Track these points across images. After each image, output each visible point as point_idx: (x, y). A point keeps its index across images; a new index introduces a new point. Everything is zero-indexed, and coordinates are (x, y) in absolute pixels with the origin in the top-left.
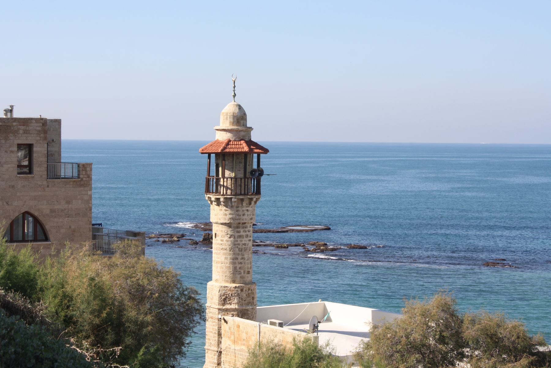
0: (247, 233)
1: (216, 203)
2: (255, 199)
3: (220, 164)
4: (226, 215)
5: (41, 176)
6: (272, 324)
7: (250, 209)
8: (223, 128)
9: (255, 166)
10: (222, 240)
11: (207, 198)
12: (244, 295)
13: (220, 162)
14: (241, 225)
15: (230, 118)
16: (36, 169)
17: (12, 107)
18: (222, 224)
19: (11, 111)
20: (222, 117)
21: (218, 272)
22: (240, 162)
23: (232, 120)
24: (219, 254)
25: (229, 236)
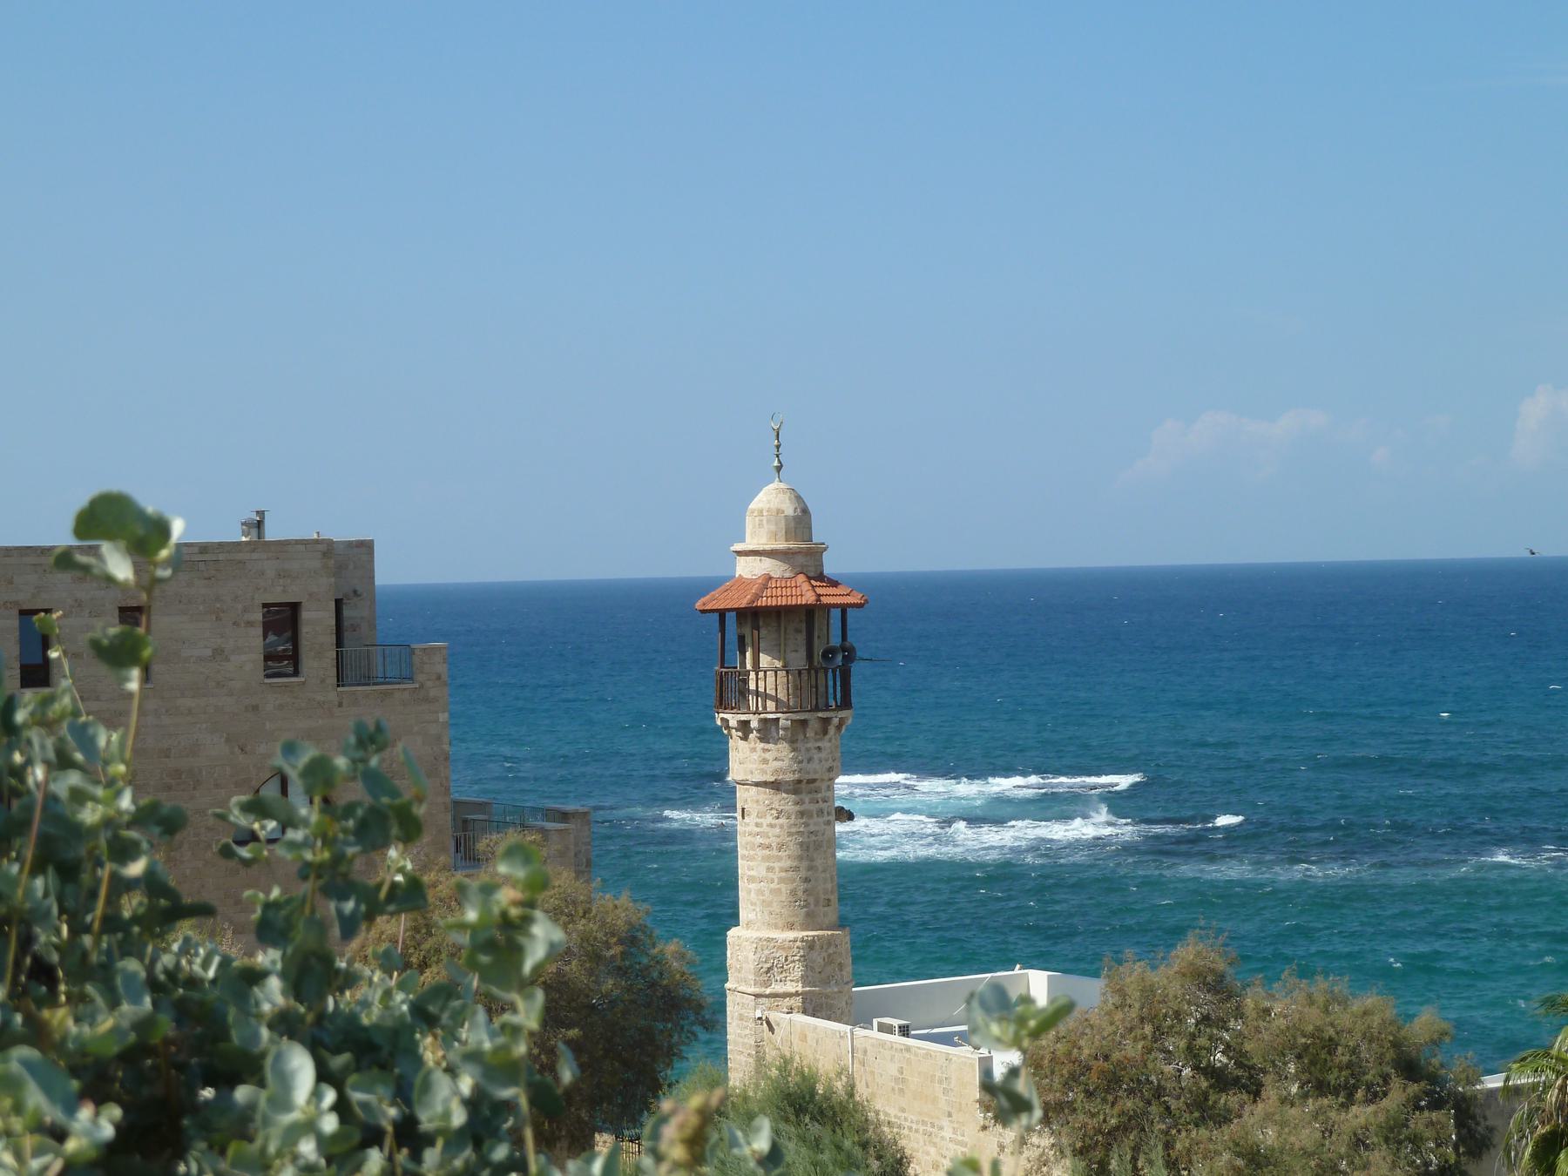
0: (821, 805)
2: (836, 721)
3: (748, 640)
5: (323, 681)
6: (884, 1028)
7: (825, 744)
8: (751, 547)
9: (836, 641)
10: (757, 825)
11: (719, 723)
12: (819, 958)
13: (747, 631)
14: (803, 786)
16: (308, 663)
17: (261, 513)
18: (757, 784)
19: (259, 525)
20: (748, 519)
22: (798, 631)
23: (773, 528)
24: (751, 859)
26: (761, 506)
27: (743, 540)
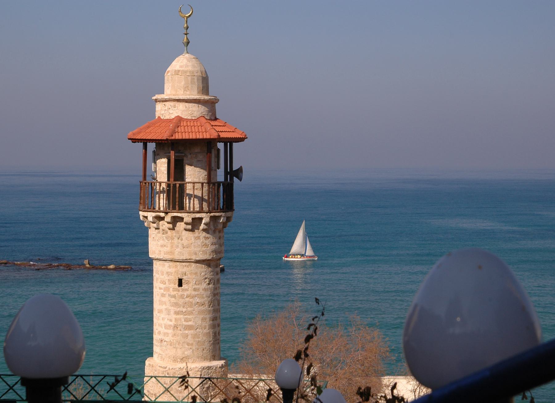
1: (189, 227)
4: (206, 245)
10: (195, 290)
15: (198, 80)
21: (188, 344)
24: (191, 313)
25: (207, 280)
26: (177, 68)
27: (163, 93)
